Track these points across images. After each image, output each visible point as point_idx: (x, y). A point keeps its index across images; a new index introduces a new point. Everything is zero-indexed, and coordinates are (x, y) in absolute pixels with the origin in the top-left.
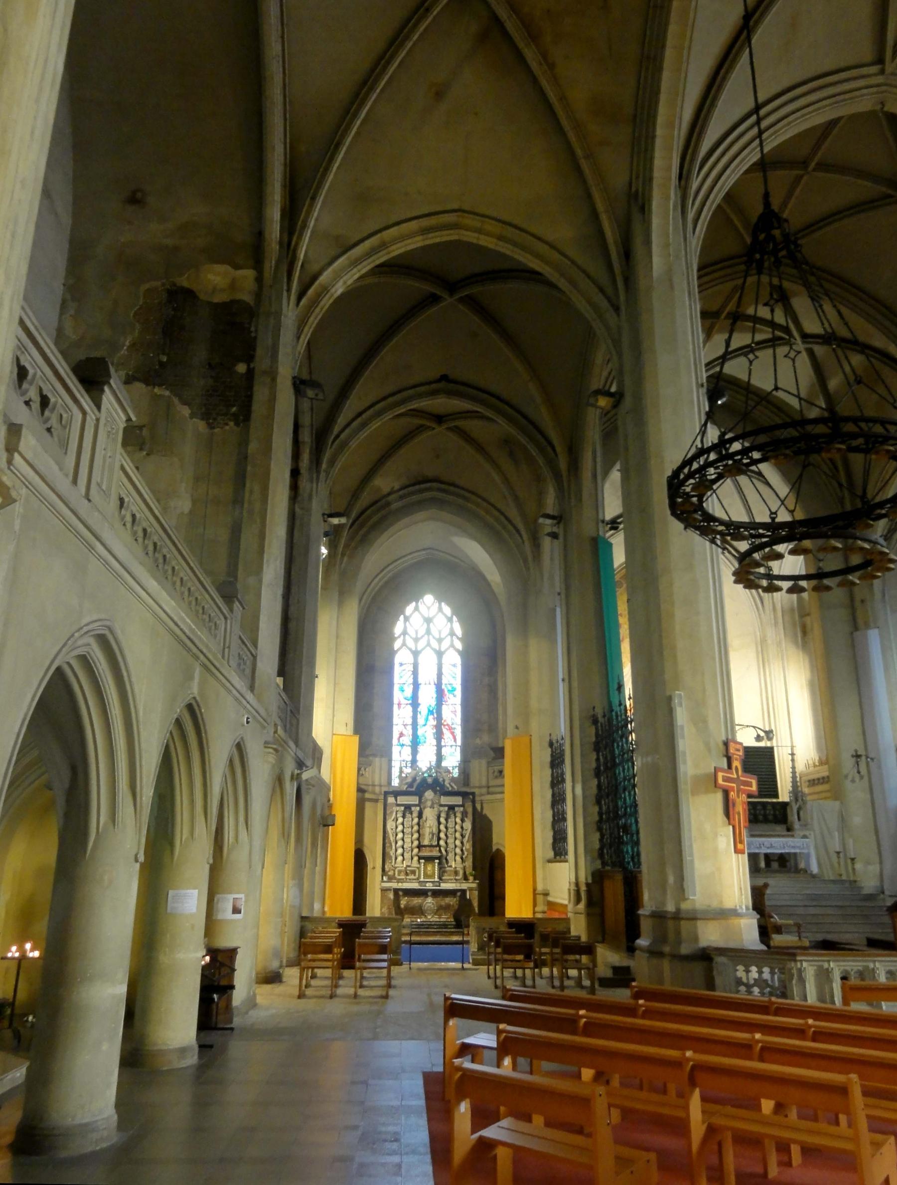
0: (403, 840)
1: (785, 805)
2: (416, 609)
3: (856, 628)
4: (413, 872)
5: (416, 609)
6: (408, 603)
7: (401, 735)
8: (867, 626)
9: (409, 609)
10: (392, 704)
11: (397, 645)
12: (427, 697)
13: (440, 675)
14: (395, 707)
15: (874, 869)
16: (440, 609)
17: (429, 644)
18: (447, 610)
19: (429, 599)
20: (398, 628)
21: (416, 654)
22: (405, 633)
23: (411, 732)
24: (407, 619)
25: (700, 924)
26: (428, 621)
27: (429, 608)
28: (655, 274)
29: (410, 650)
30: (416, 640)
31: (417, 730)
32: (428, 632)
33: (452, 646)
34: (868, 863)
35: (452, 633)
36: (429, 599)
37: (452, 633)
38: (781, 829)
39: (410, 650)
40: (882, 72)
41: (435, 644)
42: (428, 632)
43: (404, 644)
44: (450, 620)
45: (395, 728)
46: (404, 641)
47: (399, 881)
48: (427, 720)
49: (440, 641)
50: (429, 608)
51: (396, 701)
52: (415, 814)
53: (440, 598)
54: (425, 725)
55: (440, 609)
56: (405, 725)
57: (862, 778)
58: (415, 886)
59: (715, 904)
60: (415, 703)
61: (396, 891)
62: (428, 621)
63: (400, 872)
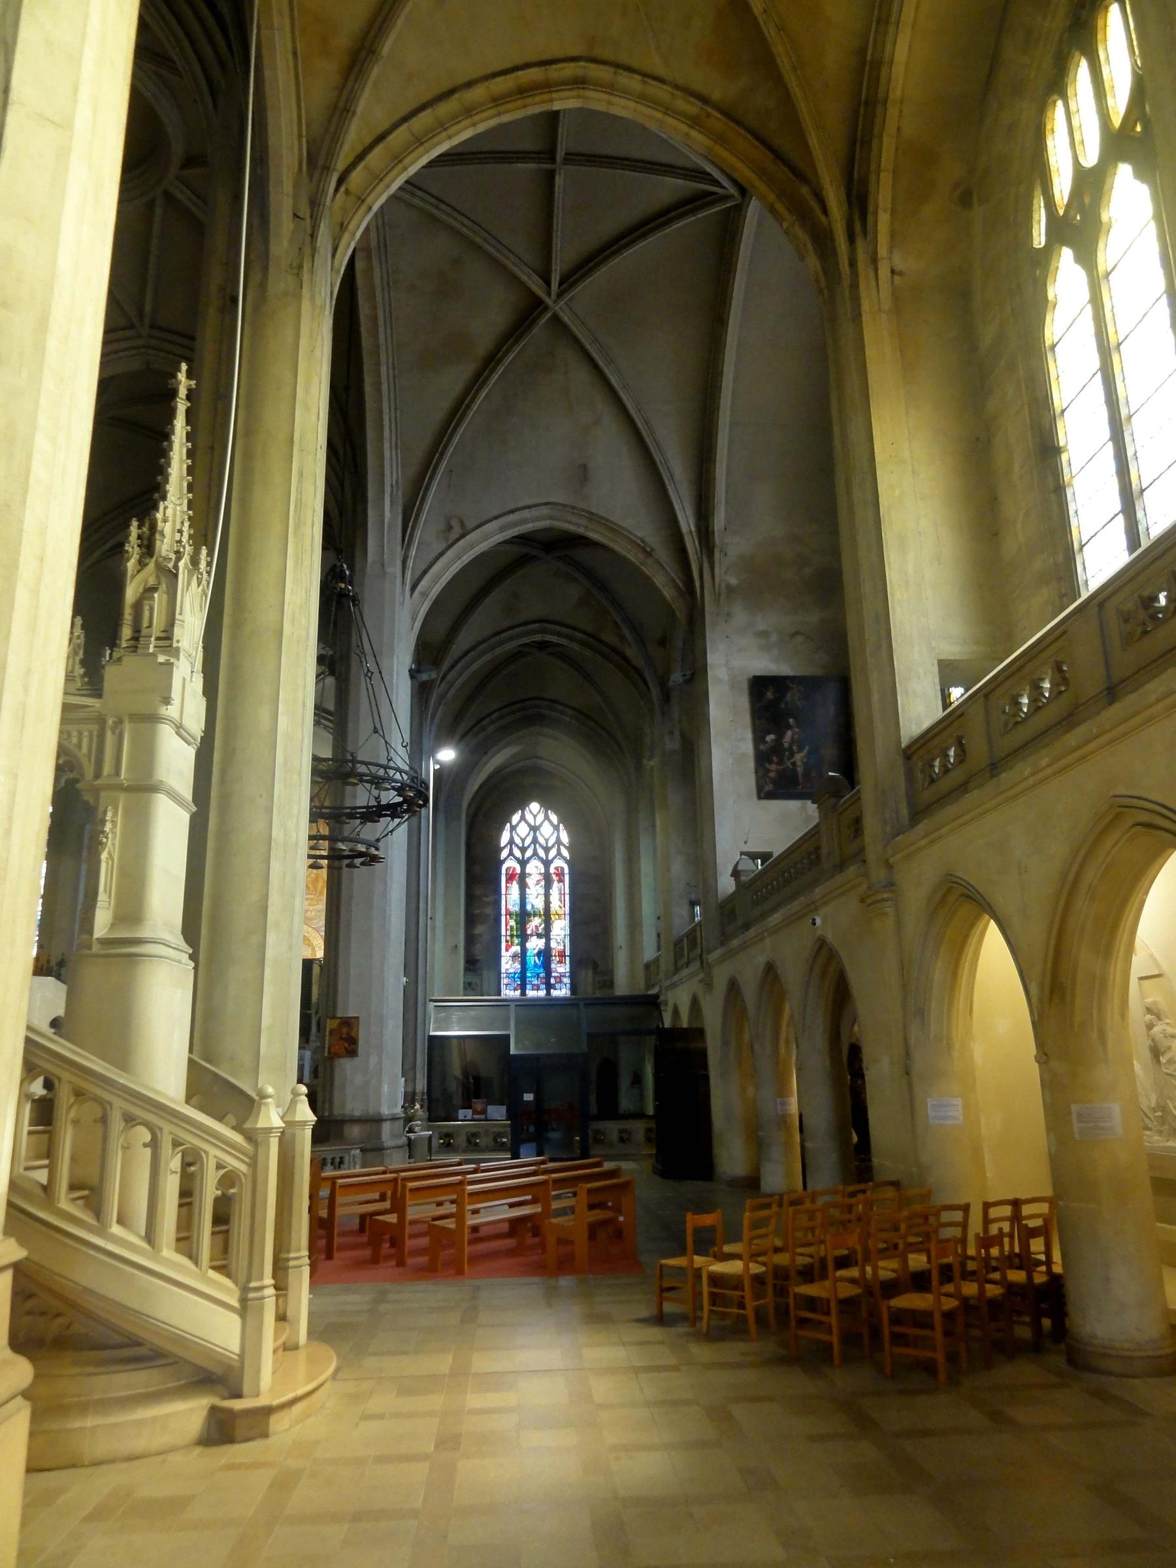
2: (523, 818)
5: (523, 818)
6: (514, 812)
9: (516, 818)
11: (504, 854)
16: (547, 817)
17: (535, 853)
18: (554, 818)
19: (535, 806)
20: (505, 838)
21: (523, 863)
22: (511, 842)
24: (513, 828)
26: (534, 829)
27: (535, 816)
29: (517, 859)
30: (523, 850)
32: (535, 841)
33: (559, 853)
36: (535, 806)
39: (517, 859)
41: (541, 853)
42: (535, 841)
43: (511, 853)
44: (556, 828)
46: (511, 850)
50: (535, 816)
53: (547, 805)
55: (547, 817)
62: (534, 829)
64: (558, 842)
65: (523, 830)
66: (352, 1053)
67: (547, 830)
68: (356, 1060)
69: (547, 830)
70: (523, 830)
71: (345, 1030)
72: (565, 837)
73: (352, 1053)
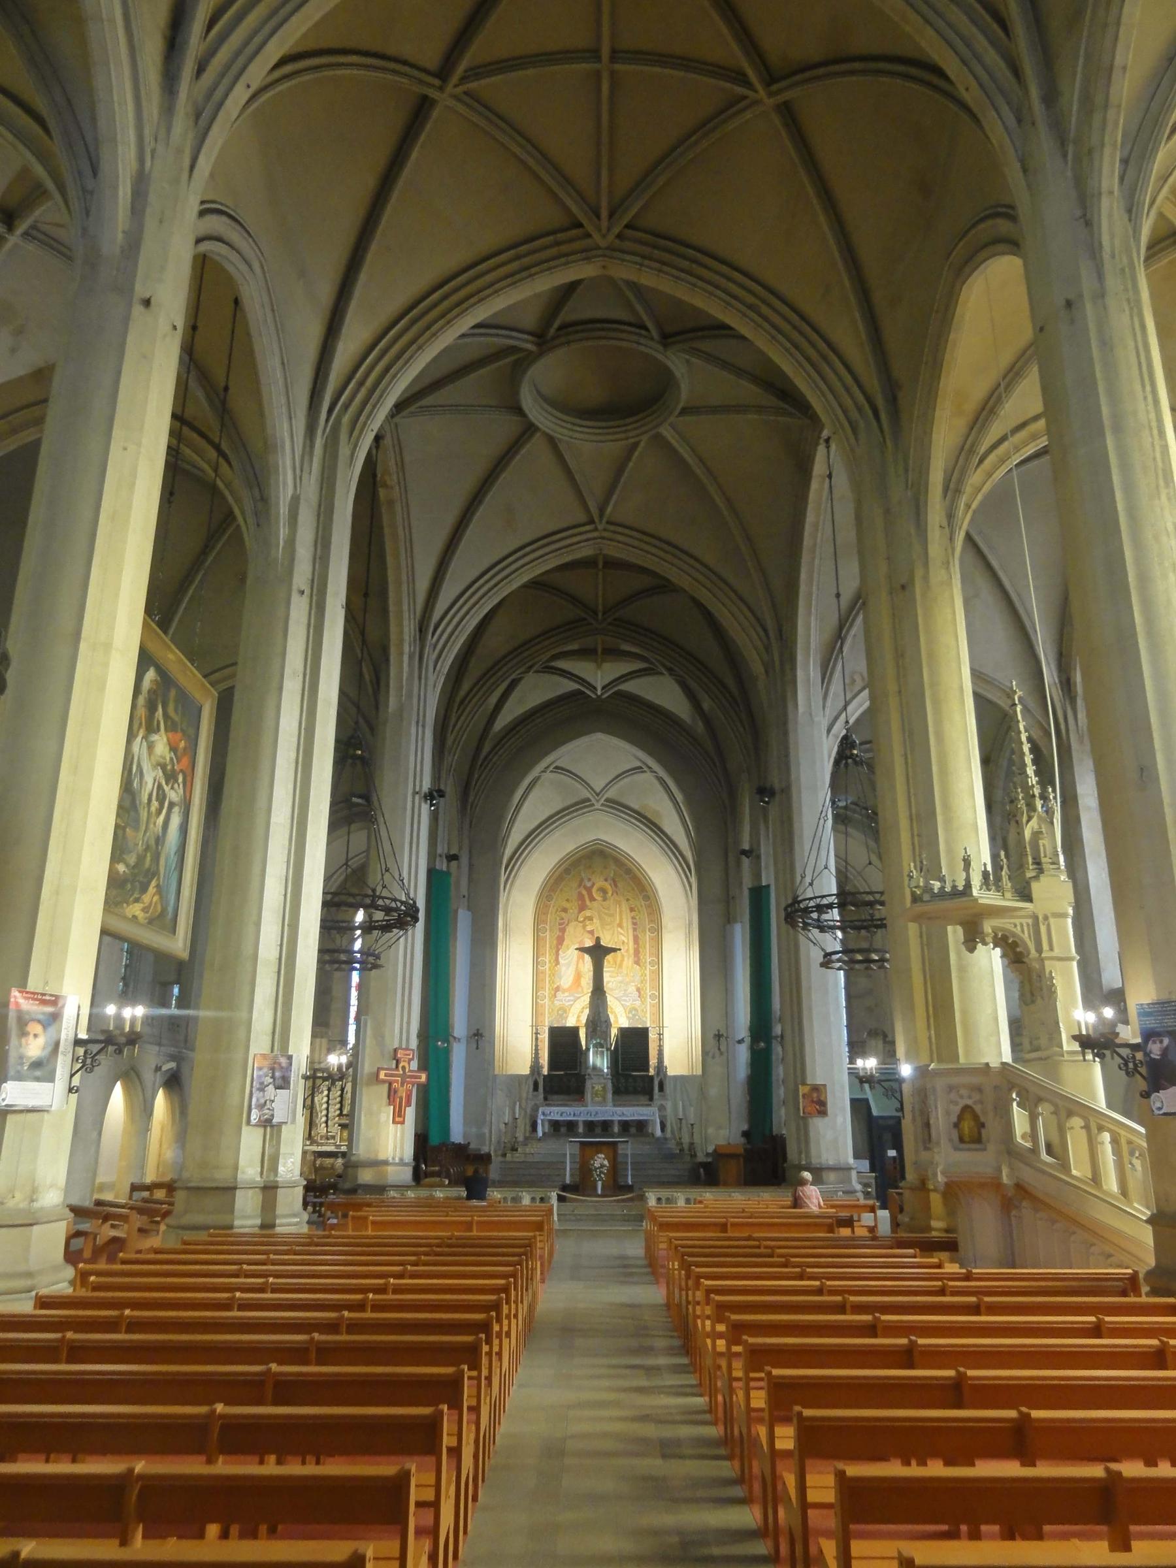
0: (327, 1109)
1: (652, 1078)
3: (729, 922)
4: (333, 1137)
8: (735, 921)
15: (724, 1133)
25: (360, 1169)
28: (390, 710)
34: (720, 1127)
38: (644, 1099)
40: (596, 529)
47: (319, 1144)
52: (338, 1088)
57: (721, 1054)
58: (332, 1148)
59: (372, 1157)
61: (314, 1152)
63: (322, 1137)
66: (823, 1113)
68: (826, 1119)
71: (815, 1095)
73: (823, 1113)
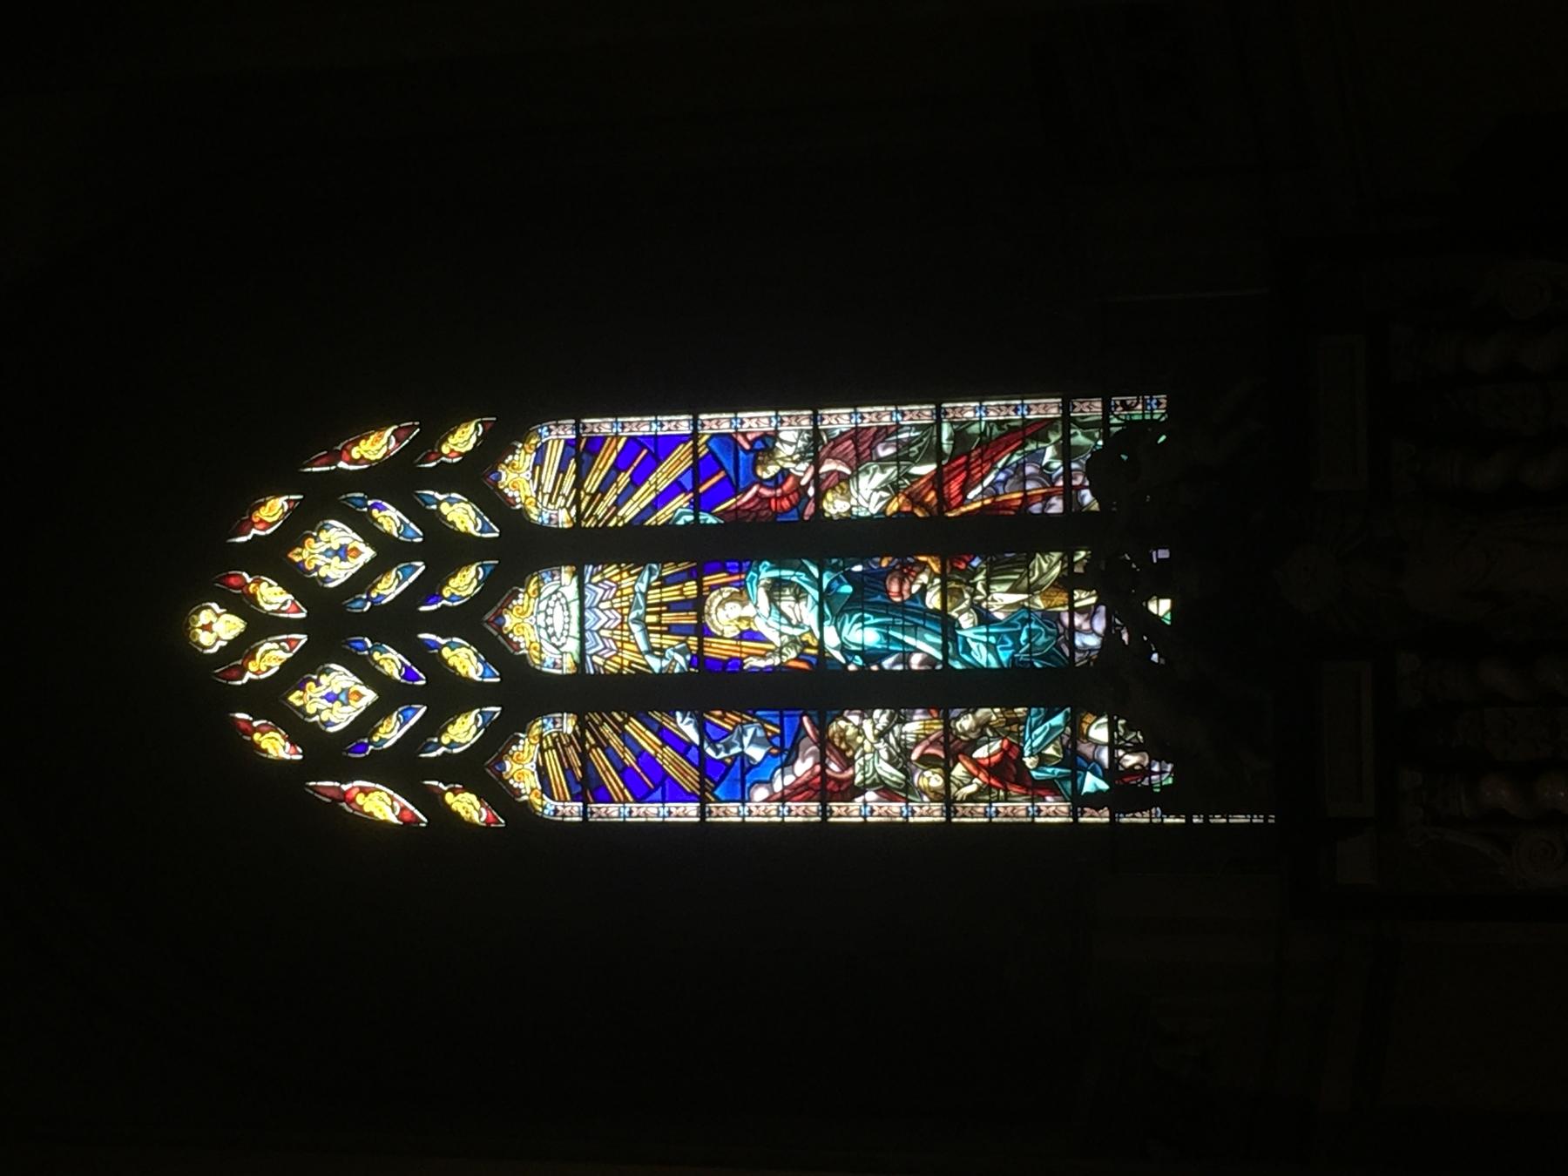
5: (271, 700)
7: (1007, 772)
10: (823, 831)
11: (467, 805)
12: (765, 618)
13: (633, 545)
14: (849, 812)
19: (216, 628)
20: (381, 804)
21: (523, 692)
22: (400, 769)
23: (993, 714)
26: (333, 626)
27: (261, 626)
30: (449, 696)
31: (976, 673)
32: (396, 625)
33: (474, 478)
35: (394, 480)
37: (394, 480)
42: (396, 625)
45: (975, 815)
48: (911, 614)
49: (446, 550)
50: (261, 626)
51: (803, 812)
54: (948, 628)
55: (274, 557)
56: (952, 749)
60: (809, 694)
62: (333, 626)
64: (399, 480)
65: (334, 699)
67: (333, 554)
69: (333, 554)
70: (334, 699)
72: (375, 447)
